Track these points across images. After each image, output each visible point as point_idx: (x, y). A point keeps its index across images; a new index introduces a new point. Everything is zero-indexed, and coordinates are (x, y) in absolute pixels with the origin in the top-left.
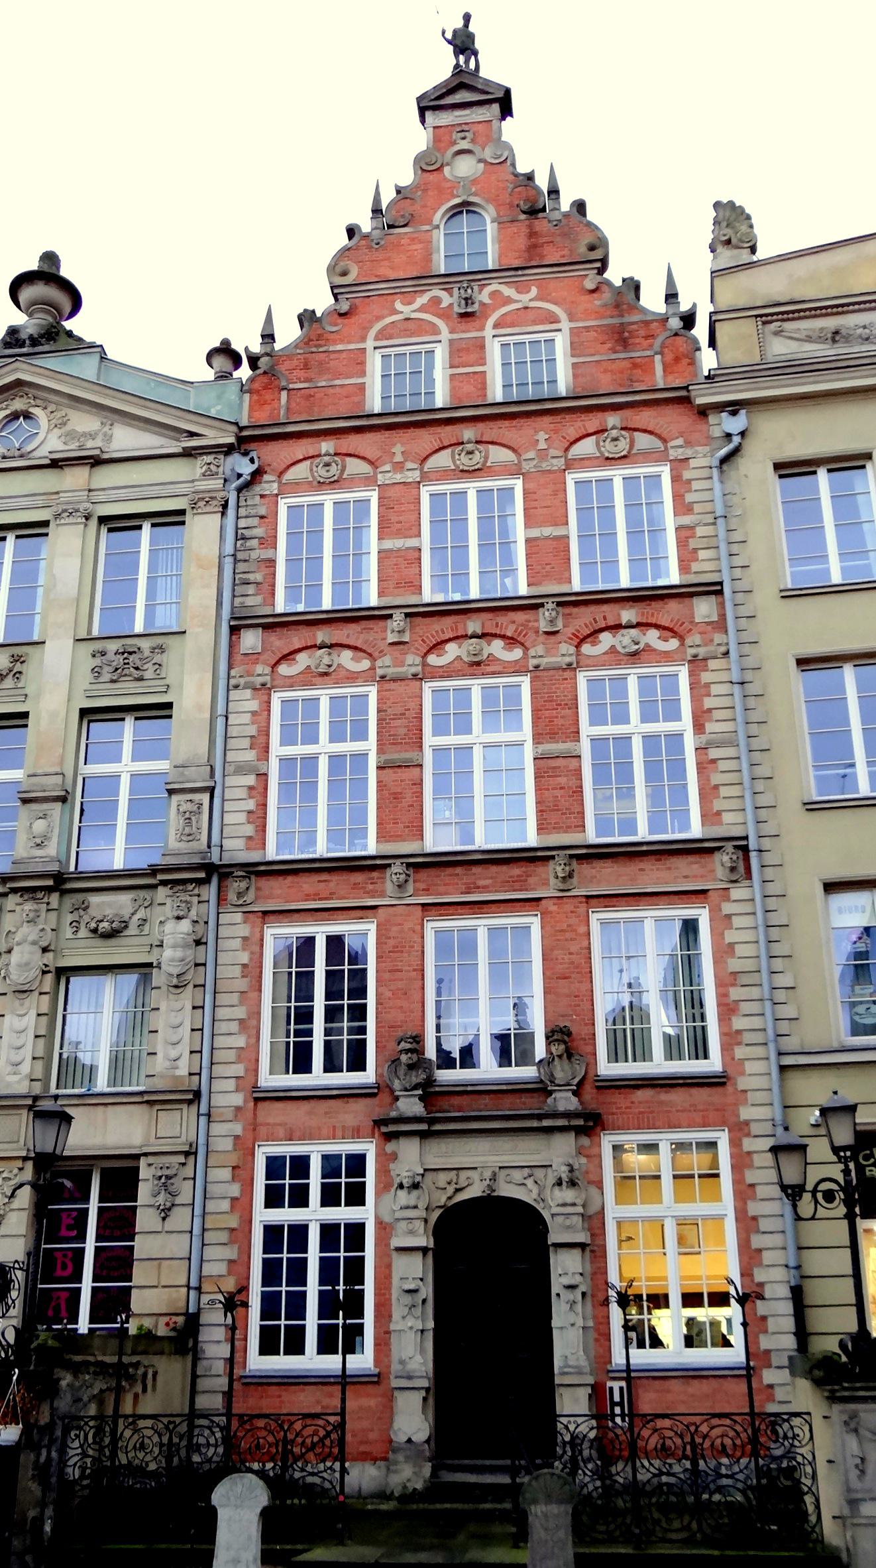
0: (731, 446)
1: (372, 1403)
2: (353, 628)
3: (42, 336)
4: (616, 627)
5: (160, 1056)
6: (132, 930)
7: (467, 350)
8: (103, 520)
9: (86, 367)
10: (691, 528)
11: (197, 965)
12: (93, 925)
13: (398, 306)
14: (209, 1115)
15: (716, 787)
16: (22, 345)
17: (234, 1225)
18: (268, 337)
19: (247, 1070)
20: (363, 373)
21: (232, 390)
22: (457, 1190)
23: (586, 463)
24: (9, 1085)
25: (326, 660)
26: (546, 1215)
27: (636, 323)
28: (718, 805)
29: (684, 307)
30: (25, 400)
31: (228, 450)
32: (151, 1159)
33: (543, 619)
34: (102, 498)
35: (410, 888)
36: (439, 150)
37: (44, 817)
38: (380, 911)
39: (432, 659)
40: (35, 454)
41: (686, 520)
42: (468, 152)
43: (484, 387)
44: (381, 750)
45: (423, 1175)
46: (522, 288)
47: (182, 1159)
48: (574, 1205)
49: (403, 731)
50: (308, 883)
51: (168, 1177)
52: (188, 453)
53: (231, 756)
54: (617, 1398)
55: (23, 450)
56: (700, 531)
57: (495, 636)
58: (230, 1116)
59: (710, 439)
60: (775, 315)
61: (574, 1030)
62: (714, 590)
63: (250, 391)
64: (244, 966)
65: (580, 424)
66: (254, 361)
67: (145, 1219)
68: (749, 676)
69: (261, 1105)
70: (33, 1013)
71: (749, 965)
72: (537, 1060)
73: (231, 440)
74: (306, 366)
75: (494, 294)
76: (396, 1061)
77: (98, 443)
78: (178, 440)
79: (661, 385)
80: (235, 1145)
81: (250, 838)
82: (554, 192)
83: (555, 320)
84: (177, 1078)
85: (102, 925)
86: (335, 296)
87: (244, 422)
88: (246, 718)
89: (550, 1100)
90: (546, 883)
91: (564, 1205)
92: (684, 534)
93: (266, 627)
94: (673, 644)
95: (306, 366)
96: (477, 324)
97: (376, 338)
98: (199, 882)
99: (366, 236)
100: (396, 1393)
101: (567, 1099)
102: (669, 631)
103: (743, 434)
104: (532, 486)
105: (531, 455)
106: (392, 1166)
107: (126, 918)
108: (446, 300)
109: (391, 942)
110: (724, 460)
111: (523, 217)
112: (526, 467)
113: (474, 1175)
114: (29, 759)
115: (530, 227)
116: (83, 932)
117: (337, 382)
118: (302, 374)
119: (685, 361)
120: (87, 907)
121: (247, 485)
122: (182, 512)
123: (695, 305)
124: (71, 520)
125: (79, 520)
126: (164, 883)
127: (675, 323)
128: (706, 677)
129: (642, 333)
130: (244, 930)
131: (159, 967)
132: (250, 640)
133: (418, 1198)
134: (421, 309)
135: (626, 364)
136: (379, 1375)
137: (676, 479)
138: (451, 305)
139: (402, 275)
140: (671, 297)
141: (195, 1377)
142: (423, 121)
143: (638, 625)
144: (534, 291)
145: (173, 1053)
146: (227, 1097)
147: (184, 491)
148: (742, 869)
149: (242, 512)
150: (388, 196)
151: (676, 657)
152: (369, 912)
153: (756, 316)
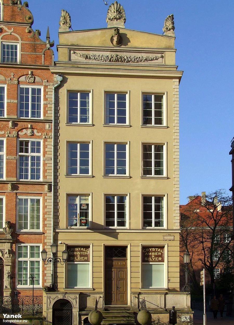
4: (27, 128)
10: (47, 104)
26: (3, 259)
27: (39, 44)
46: (9, 29)
54: (16, 294)
65: (22, 72)
72: (3, 227)
92: (45, 105)
94: (40, 134)
101: (9, 236)
104: (9, 88)
123: (54, 41)
135: (35, 56)
137: (45, 91)
144: (12, 29)
151: (41, 137)
153: (68, 48)
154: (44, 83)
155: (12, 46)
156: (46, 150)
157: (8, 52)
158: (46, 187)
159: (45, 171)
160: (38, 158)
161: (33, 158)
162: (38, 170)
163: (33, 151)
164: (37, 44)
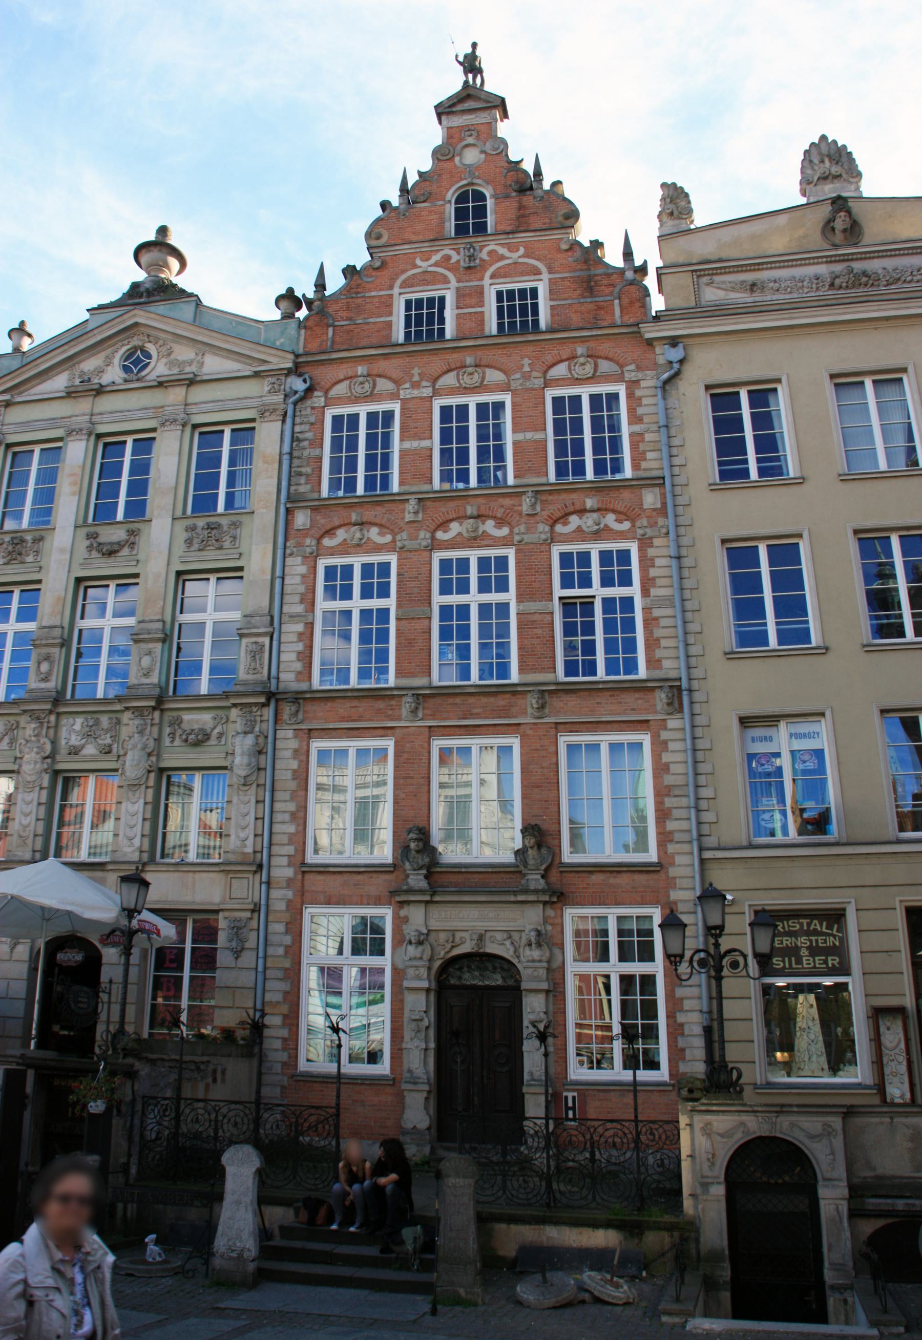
0: (672, 372)
1: (390, 1099)
2: (379, 510)
4: (582, 512)
5: (233, 837)
6: (213, 741)
7: (470, 295)
8: (195, 427)
9: (186, 311)
10: (641, 435)
11: (259, 769)
12: (184, 737)
13: (418, 262)
14: (268, 883)
15: (658, 640)
16: (141, 297)
17: (288, 965)
18: (320, 285)
19: (296, 850)
20: (391, 314)
21: (293, 324)
22: (453, 947)
23: (561, 383)
24: (125, 854)
25: (358, 535)
26: (519, 966)
28: (658, 654)
29: (638, 262)
30: (141, 337)
31: (289, 372)
32: (227, 914)
33: (526, 504)
34: (194, 410)
35: (420, 715)
36: (451, 145)
37: (149, 653)
38: (398, 731)
39: (440, 535)
40: (148, 378)
41: (637, 428)
42: (474, 145)
43: (481, 322)
44: (399, 606)
45: (427, 935)
46: (512, 248)
47: (248, 914)
48: (540, 961)
49: (416, 590)
50: (343, 708)
51: (239, 928)
52: (257, 375)
53: (286, 609)
56: (648, 437)
57: (488, 517)
58: (284, 885)
59: (655, 366)
60: (704, 270)
61: (544, 826)
62: (658, 482)
63: (305, 328)
64: (295, 771)
66: (310, 303)
67: (223, 958)
68: (684, 552)
69: (307, 876)
70: (142, 801)
71: (680, 780)
73: (290, 365)
74: (348, 308)
75: (490, 253)
76: (407, 848)
77: (193, 368)
78: (250, 365)
79: (619, 323)
80: (288, 906)
81: (299, 673)
82: (538, 173)
83: (539, 273)
84: (244, 854)
85: (192, 737)
86: (371, 254)
87: (301, 351)
88: (298, 579)
89: (523, 882)
90: (524, 713)
91: (533, 961)
92: (636, 439)
93: (314, 509)
94: (626, 525)
95: (348, 308)
96: (478, 275)
97: (401, 287)
98: (264, 705)
99: (397, 208)
100: (406, 1093)
101: (537, 880)
102: (622, 515)
103: (681, 362)
104: (518, 400)
105: (518, 376)
106: (404, 927)
107: (209, 731)
108: (455, 257)
109: (405, 756)
110: (666, 382)
111: (514, 194)
112: (514, 385)
113: (466, 935)
114: (139, 612)
115: (520, 202)
116: (177, 742)
117: (371, 320)
118: (345, 314)
119: (638, 304)
120: (181, 722)
121: (302, 399)
122: (253, 420)
123: (645, 262)
124: (173, 427)
126: (235, 705)
127: (629, 275)
128: (651, 552)
129: (604, 282)
130: (294, 744)
131: (231, 769)
132: (301, 519)
133: (423, 951)
134: (436, 264)
135: (592, 306)
136: (394, 1079)
137: (630, 395)
138: (458, 261)
139: (421, 238)
140: (628, 254)
141: (260, 1074)
142: (440, 123)
143: (599, 510)
144: (522, 251)
145: (242, 835)
146: (282, 871)
147: (255, 404)
148: (675, 703)
149: (298, 420)
150: (413, 179)
152: (389, 732)
153: (692, 271)
154: (626, 375)
155: (522, 292)
156: (653, 572)
157: (511, 309)
158: (661, 697)
159: (652, 644)
160: (628, 603)
161: (608, 603)
162: (630, 645)
163: (607, 581)
164: (596, 275)
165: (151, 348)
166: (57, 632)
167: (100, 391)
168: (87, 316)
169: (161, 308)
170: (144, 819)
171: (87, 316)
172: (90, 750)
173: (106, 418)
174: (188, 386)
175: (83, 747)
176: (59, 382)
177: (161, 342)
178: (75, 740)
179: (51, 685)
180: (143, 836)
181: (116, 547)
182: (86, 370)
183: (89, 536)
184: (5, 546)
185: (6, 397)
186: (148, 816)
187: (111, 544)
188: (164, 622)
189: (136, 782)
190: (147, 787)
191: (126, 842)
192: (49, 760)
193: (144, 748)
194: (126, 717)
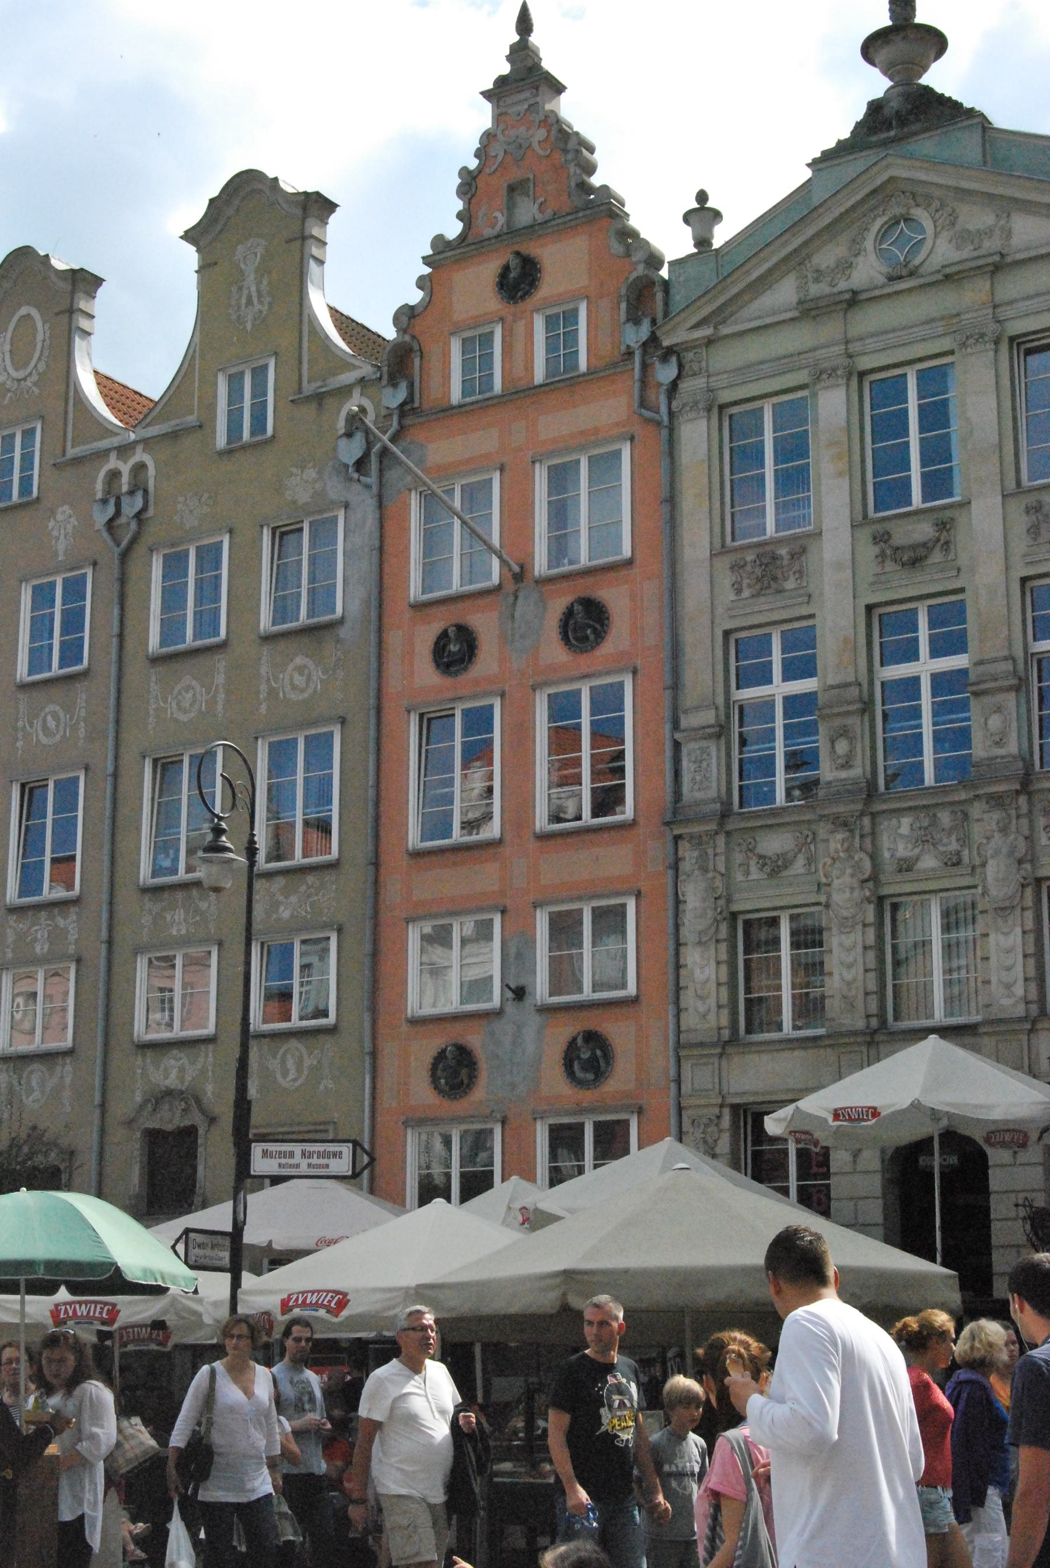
3: (910, 112)
8: (1012, 339)
9: (967, 145)
16: (890, 127)
37: (999, 710)
55: (911, 266)
125: (988, 346)
165: (921, 214)
166: (854, 692)
167: (854, 300)
168: (808, 173)
169: (926, 145)
170: (1025, 956)
171: (808, 173)
172: (929, 862)
173: (871, 344)
174: (993, 273)
175: (917, 859)
176: (784, 294)
177: (936, 204)
178: (903, 850)
179: (856, 772)
180: (1026, 979)
181: (921, 552)
182: (823, 267)
183: (877, 539)
184: (748, 568)
185: (707, 331)
186: (1031, 950)
187: (913, 547)
188: (1014, 660)
189: (1007, 904)
190: (1023, 909)
191: (1002, 990)
192: (871, 884)
193: (1011, 854)
194: (976, 810)
